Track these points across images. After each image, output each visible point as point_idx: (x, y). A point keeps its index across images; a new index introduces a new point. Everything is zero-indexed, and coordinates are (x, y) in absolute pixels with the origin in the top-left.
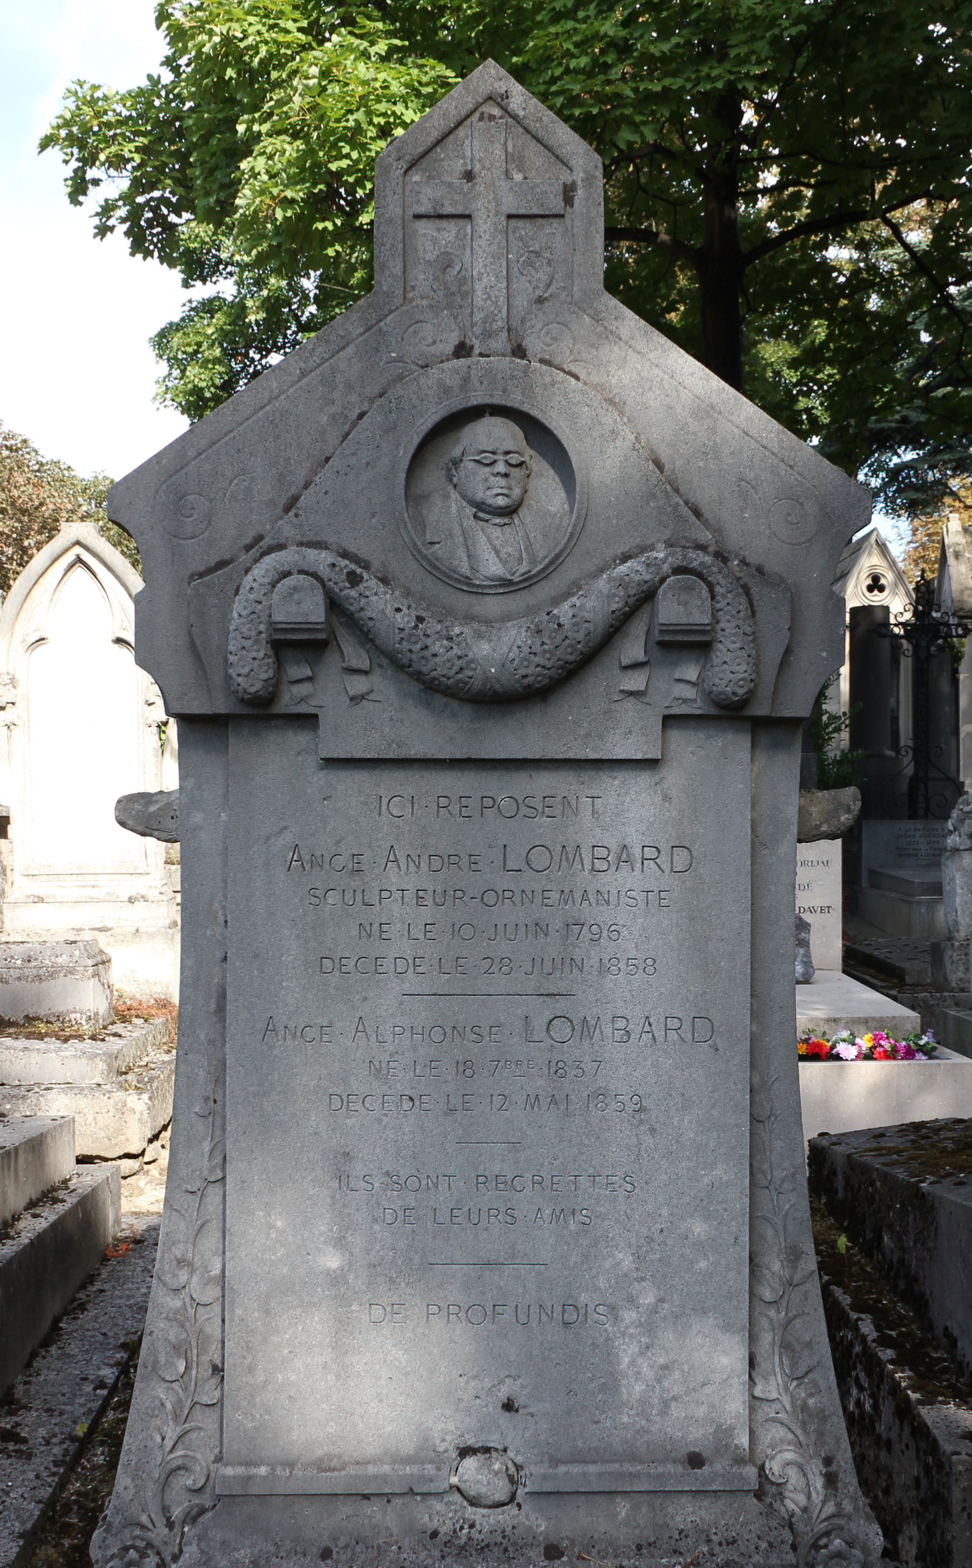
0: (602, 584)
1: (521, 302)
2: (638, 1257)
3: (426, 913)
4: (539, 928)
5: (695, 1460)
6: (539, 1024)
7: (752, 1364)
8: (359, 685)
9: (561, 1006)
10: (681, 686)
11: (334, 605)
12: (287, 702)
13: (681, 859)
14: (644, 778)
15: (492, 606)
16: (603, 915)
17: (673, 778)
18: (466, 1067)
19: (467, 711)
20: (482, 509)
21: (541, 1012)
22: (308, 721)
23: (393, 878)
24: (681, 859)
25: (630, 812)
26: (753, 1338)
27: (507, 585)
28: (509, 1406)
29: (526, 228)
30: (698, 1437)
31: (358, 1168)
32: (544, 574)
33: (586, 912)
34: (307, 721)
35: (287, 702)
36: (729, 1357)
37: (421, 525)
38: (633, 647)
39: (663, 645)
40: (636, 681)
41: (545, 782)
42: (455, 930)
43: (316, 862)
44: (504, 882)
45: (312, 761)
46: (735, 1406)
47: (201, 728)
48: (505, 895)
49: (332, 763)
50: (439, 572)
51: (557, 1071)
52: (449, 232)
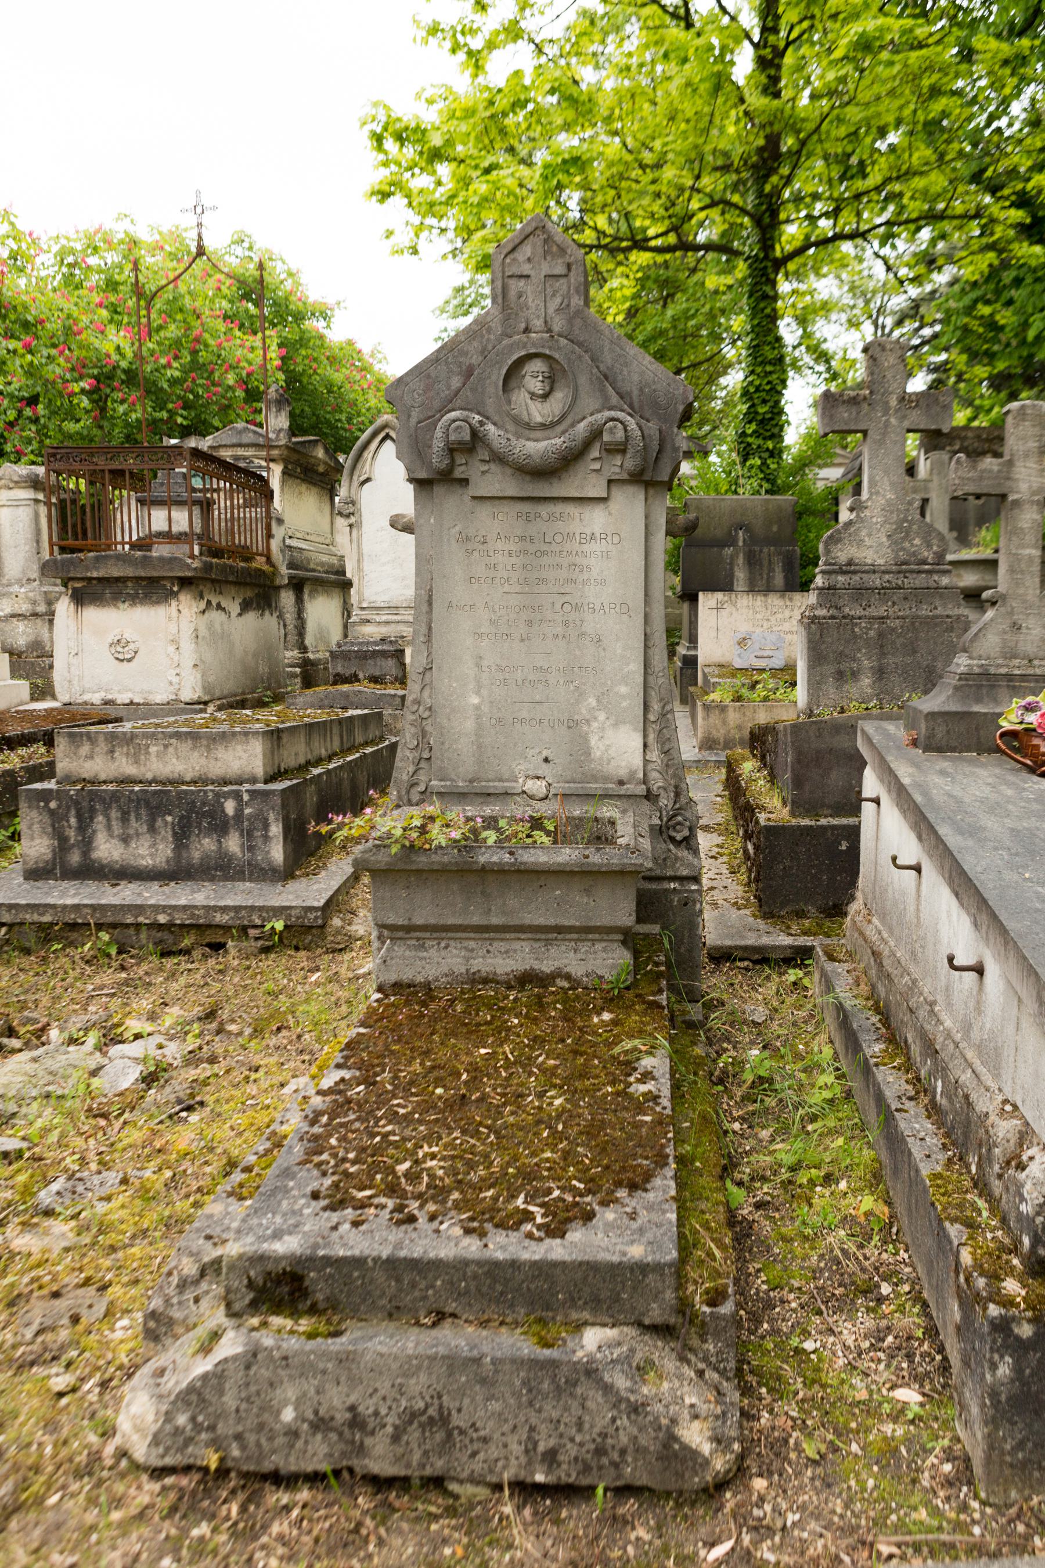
0: (582, 425)
1: (551, 311)
2: (598, 701)
3: (513, 560)
4: (559, 566)
5: (621, 783)
6: (558, 606)
7: (645, 745)
8: (485, 468)
9: (567, 598)
10: (615, 467)
11: (474, 433)
12: (458, 473)
13: (616, 539)
14: (602, 506)
15: (538, 434)
16: (585, 562)
17: (614, 505)
18: (529, 623)
19: (528, 478)
20: (533, 395)
21: (559, 601)
22: (464, 482)
23: (499, 545)
24: (616, 539)
25: (596, 520)
26: (645, 736)
27: (543, 426)
28: (546, 760)
29: (551, 281)
30: (623, 773)
31: (485, 663)
32: (559, 422)
33: (579, 560)
34: (464, 482)
35: (458, 473)
36: (636, 741)
37: (509, 402)
38: (595, 453)
39: (608, 451)
40: (597, 466)
41: (559, 508)
42: (524, 566)
43: (468, 539)
44: (544, 547)
45: (467, 499)
46: (637, 761)
47: (421, 485)
48: (544, 553)
49: (474, 498)
50: (517, 421)
51: (566, 624)
52: (522, 283)
